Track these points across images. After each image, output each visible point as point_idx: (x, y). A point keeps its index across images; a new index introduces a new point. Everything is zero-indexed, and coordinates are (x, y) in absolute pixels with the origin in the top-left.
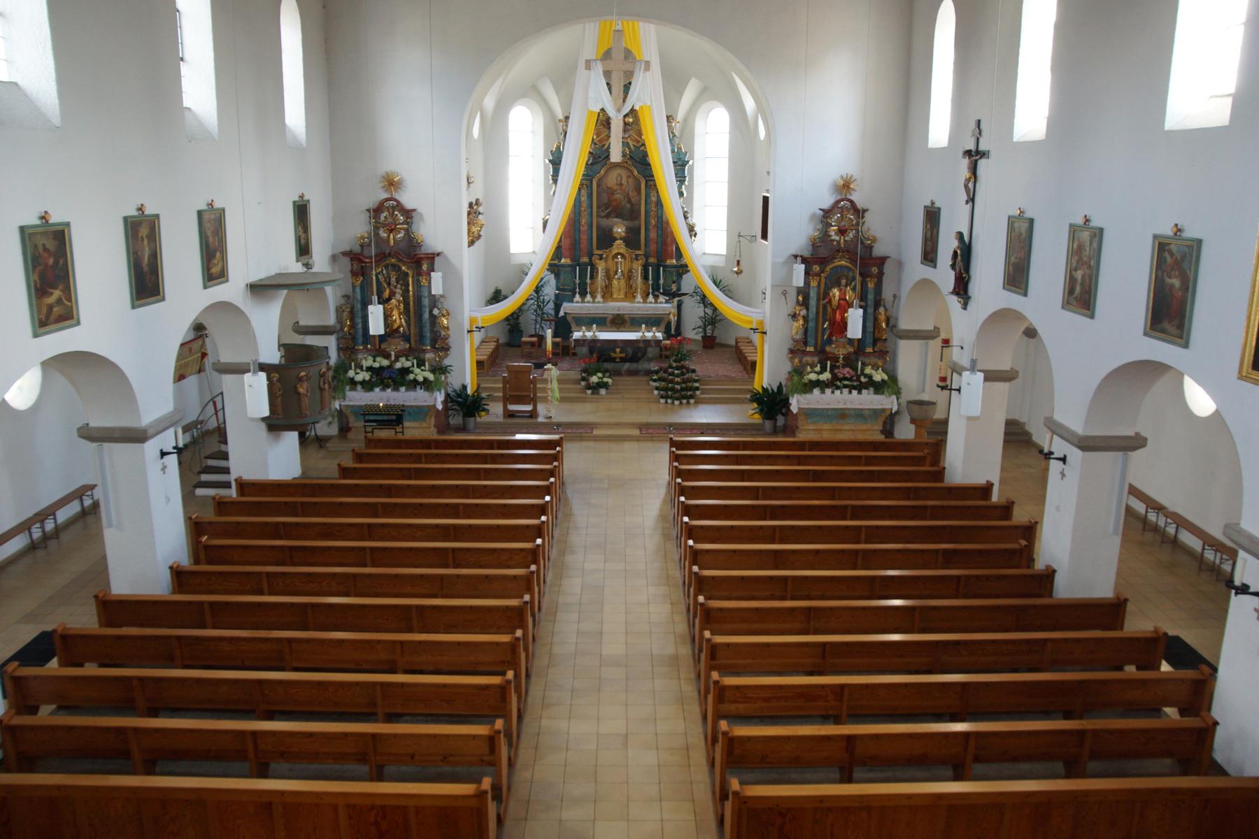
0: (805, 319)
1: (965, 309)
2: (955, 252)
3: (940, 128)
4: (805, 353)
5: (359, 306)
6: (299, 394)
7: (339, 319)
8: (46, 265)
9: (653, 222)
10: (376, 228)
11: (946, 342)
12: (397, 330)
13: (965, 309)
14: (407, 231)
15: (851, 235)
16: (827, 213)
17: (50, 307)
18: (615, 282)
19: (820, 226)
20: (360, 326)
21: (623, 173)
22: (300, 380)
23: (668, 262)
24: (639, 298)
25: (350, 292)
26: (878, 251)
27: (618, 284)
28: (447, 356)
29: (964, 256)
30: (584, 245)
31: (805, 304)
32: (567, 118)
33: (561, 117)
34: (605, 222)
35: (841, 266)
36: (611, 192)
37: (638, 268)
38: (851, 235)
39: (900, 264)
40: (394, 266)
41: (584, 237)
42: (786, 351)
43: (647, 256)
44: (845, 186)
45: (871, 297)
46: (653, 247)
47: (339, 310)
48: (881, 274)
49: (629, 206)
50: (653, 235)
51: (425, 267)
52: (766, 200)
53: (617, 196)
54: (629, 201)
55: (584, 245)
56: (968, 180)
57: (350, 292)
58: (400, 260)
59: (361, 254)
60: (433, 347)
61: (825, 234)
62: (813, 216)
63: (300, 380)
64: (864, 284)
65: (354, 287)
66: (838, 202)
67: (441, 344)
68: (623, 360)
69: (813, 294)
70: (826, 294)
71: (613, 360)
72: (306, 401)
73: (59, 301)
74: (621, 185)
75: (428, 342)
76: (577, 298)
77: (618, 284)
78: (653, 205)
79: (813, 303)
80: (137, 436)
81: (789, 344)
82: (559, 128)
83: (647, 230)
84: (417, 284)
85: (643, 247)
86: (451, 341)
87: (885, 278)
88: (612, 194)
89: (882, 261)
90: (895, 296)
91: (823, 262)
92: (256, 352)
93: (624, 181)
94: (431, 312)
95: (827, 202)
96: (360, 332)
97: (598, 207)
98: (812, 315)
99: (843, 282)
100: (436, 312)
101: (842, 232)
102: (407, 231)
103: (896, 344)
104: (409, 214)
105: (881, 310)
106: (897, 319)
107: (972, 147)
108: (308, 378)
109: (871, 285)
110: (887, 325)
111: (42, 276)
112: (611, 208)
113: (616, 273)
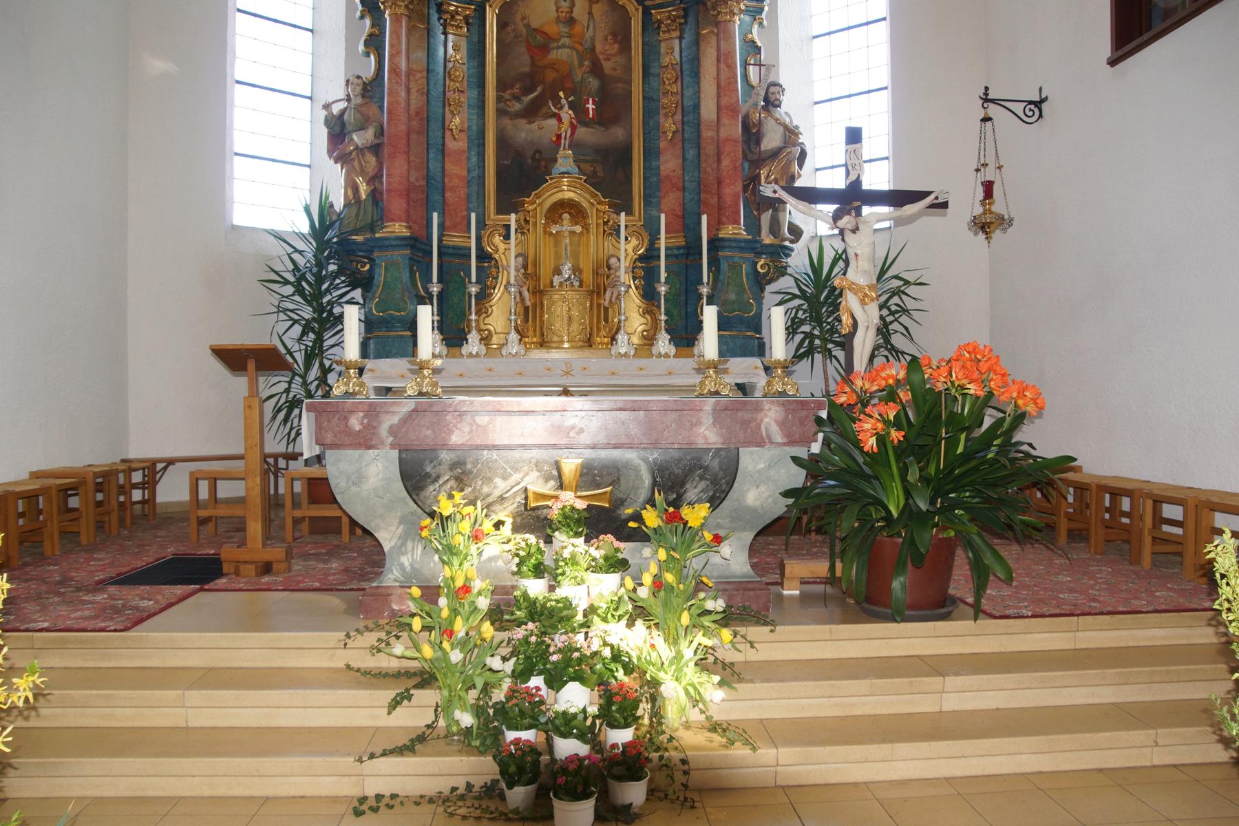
9: (669, 125)
23: (728, 231)
27: (565, 308)
36: (540, 43)
46: (671, 200)
49: (594, 83)
50: (669, 164)
53: (561, 54)
54: (596, 69)
74: (571, 21)
77: (565, 308)
78: (668, 75)
83: (651, 153)
88: (545, 49)
97: (502, 85)
113: (558, 271)
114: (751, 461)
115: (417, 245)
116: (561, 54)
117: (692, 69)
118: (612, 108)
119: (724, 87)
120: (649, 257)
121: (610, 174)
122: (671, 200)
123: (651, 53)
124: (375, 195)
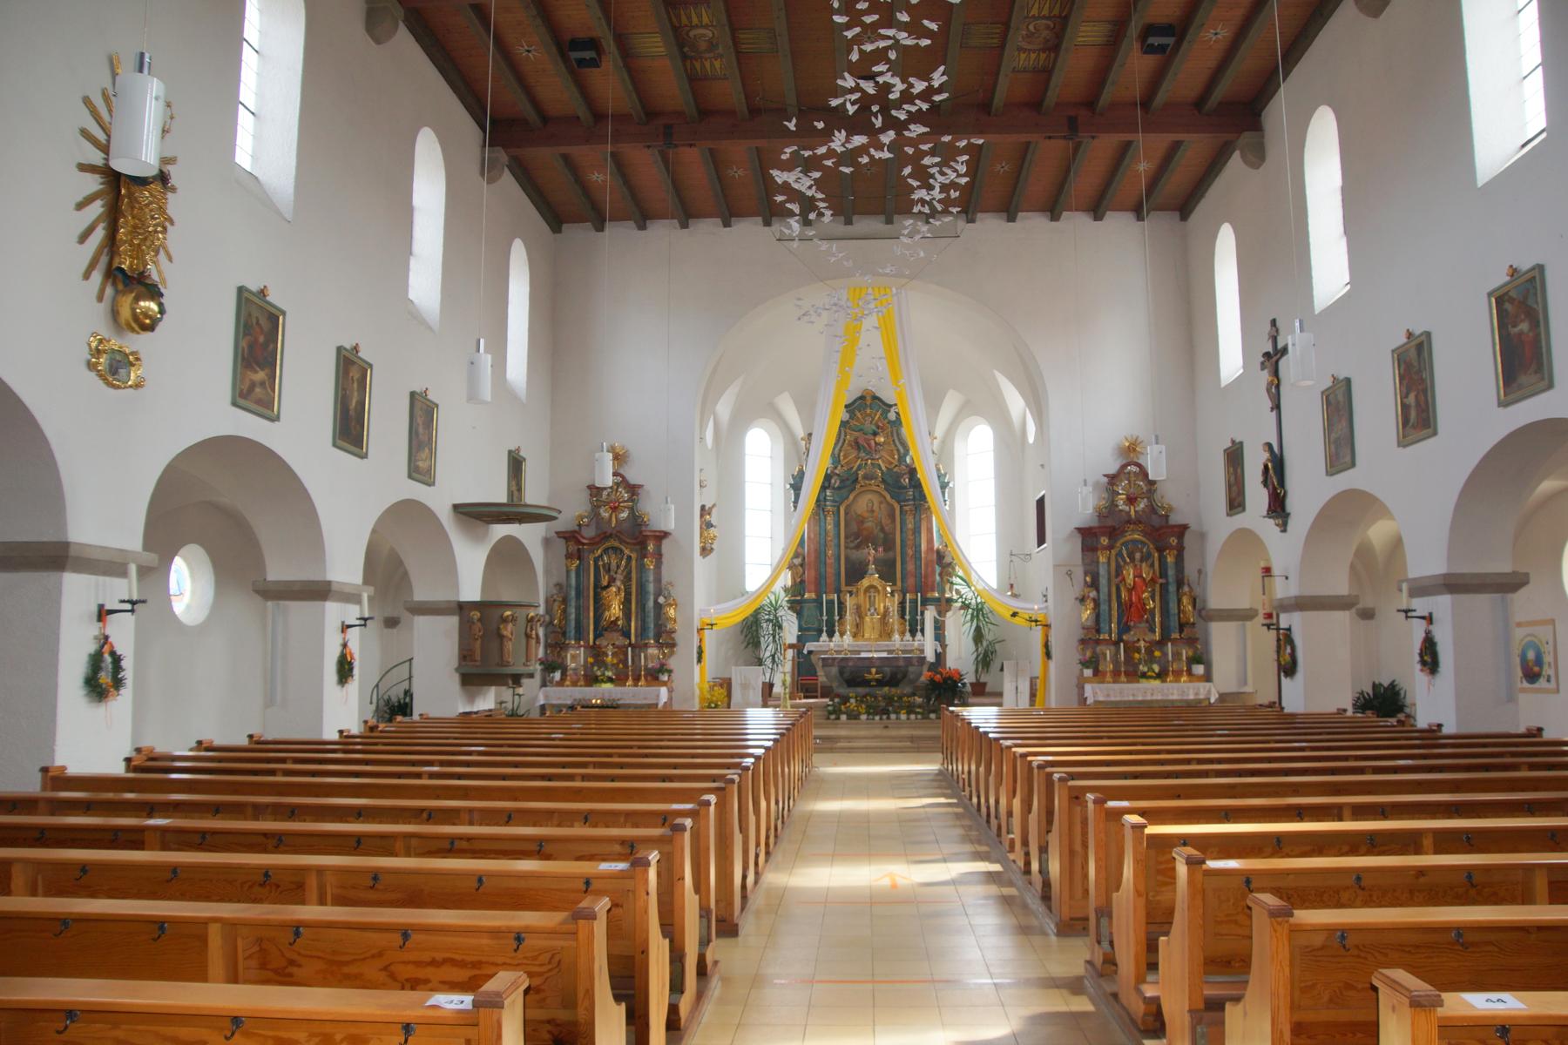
0: (1096, 602)
1: (1284, 531)
2: (1266, 467)
3: (1231, 354)
4: (1098, 642)
5: (573, 593)
6: (501, 637)
7: (549, 610)
8: (256, 340)
9: (910, 552)
10: (595, 509)
11: (1267, 571)
12: (614, 623)
13: (1284, 531)
14: (632, 509)
15: (1142, 505)
16: (1113, 479)
17: (253, 385)
18: (867, 619)
19: (1105, 495)
20: (573, 616)
21: (875, 499)
22: (505, 620)
24: (897, 636)
25: (563, 580)
26: (1175, 519)
28: (672, 653)
29: (1276, 471)
30: (831, 579)
31: (1094, 585)
32: (810, 435)
33: (800, 432)
34: (855, 555)
35: (1134, 541)
36: (861, 521)
37: (893, 605)
38: (1142, 505)
39: (1202, 536)
40: (615, 549)
41: (830, 571)
42: (1075, 643)
43: (903, 593)
44: (1130, 451)
45: (1171, 572)
46: (911, 581)
47: (549, 602)
48: (1180, 550)
50: (910, 567)
51: (651, 547)
52: (1041, 503)
53: (869, 524)
54: (882, 530)
55: (831, 579)
56: (1270, 384)
57: (563, 580)
58: (622, 541)
59: (578, 532)
60: (657, 641)
61: (1113, 504)
62: (1096, 485)
63: (505, 620)
64: (1162, 560)
65: (568, 572)
66: (1124, 466)
67: (666, 639)
68: (881, 683)
69: (1102, 571)
70: (1119, 572)
71: (866, 683)
72: (509, 646)
73: (262, 384)
75: (651, 634)
76: (824, 636)
79: (1103, 581)
80: (320, 591)
81: (1080, 634)
82: (797, 450)
84: (642, 568)
85: (899, 583)
86: (678, 637)
87: (1187, 555)
89: (1183, 528)
90: (1200, 572)
91: (1113, 533)
92: (455, 585)
93: (876, 507)
94: (656, 602)
95: (1113, 468)
96: (573, 624)
98: (1103, 596)
99: (1138, 556)
100: (661, 600)
101: (1131, 500)
102: (632, 509)
103: (1207, 633)
104: (633, 490)
105: (1186, 589)
106: (1204, 601)
107: (1269, 348)
108: (514, 619)
109: (1170, 560)
110: (1194, 607)
111: (251, 346)
112: (859, 536)
114: (911, 669)
115: (819, 601)
116: (869, 524)
117: (917, 531)
118: (888, 545)
119: (930, 541)
120: (902, 604)
121: (887, 573)
122: (911, 581)
123: (903, 523)
124: (802, 582)
